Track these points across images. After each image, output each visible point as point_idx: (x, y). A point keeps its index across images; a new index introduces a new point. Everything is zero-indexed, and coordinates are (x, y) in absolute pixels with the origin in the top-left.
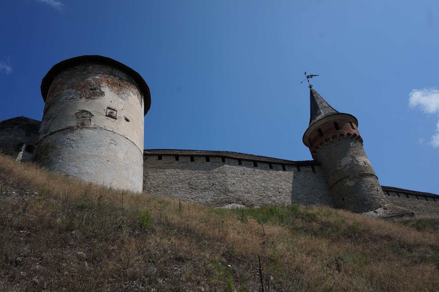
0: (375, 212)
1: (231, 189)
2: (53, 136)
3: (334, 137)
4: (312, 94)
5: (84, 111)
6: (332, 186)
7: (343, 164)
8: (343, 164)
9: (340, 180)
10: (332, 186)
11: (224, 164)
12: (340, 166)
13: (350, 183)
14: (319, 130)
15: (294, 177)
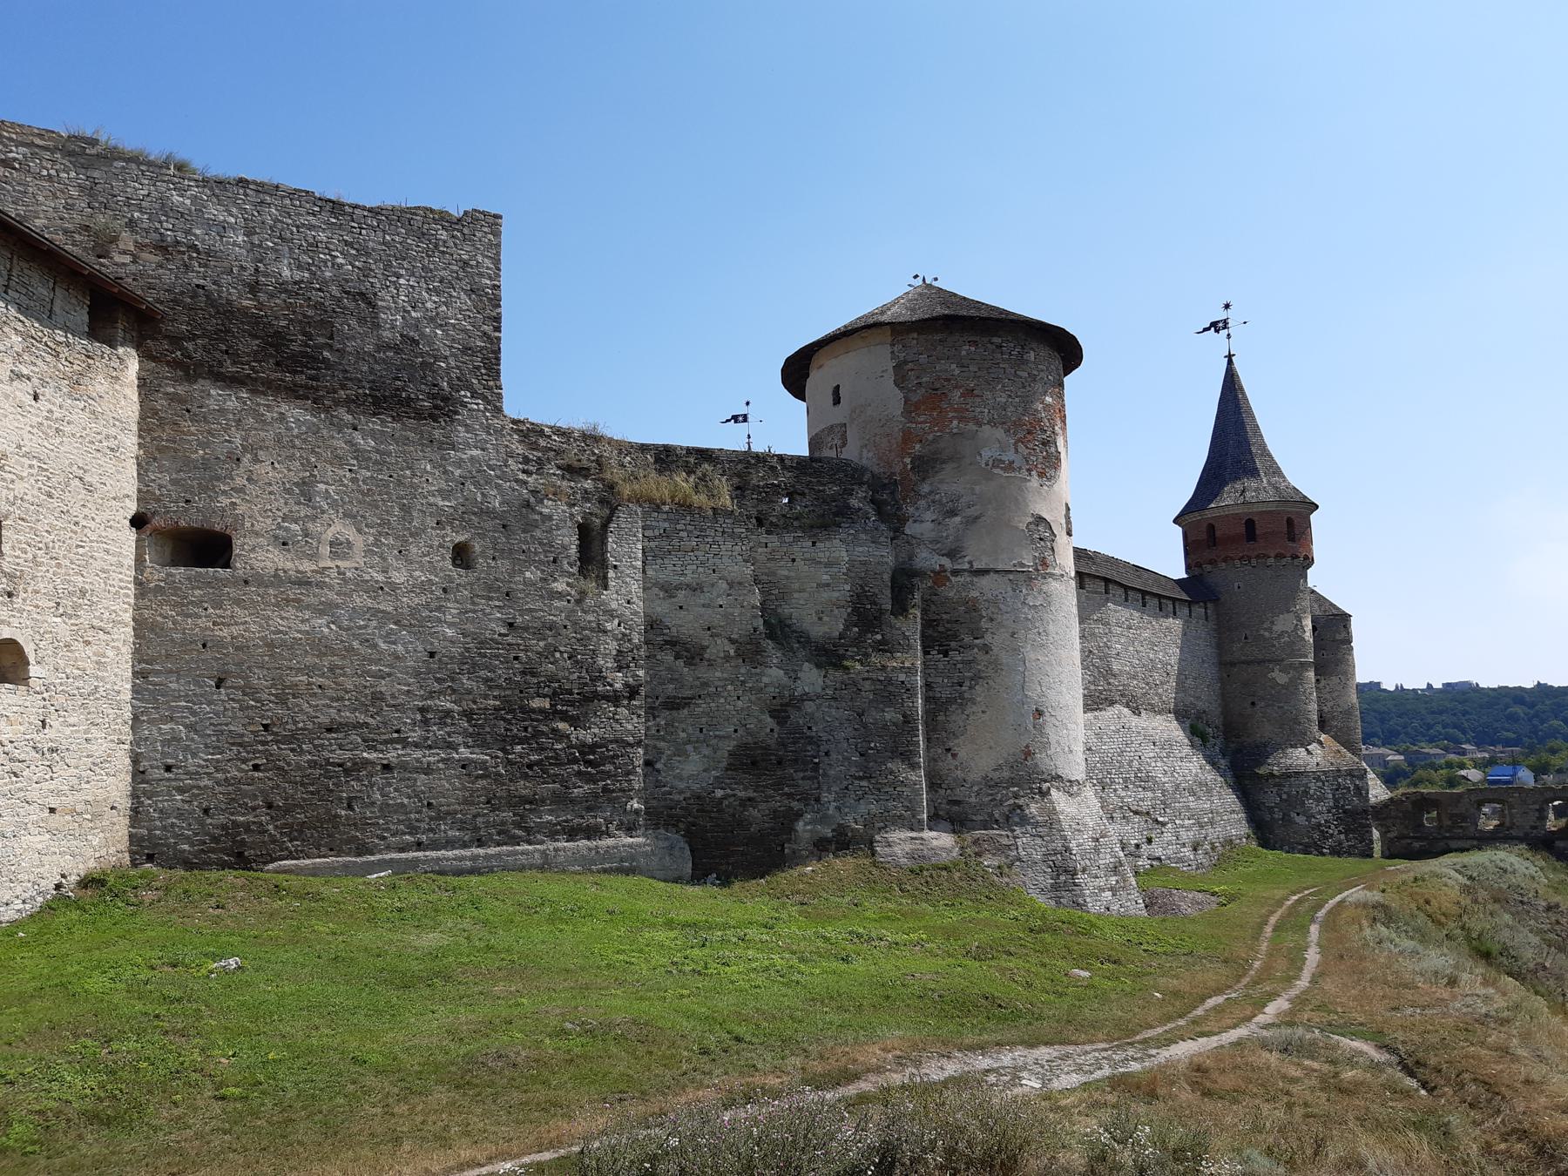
0: (1309, 752)
1: (1116, 667)
2: (985, 582)
3: (1279, 556)
4: (1231, 385)
5: (1040, 520)
6: (1233, 664)
7: (1278, 628)
8: (1278, 628)
9: (1261, 662)
10: (1233, 664)
11: (1107, 600)
12: (1270, 630)
13: (1281, 678)
14: (1250, 524)
15: (1185, 634)
